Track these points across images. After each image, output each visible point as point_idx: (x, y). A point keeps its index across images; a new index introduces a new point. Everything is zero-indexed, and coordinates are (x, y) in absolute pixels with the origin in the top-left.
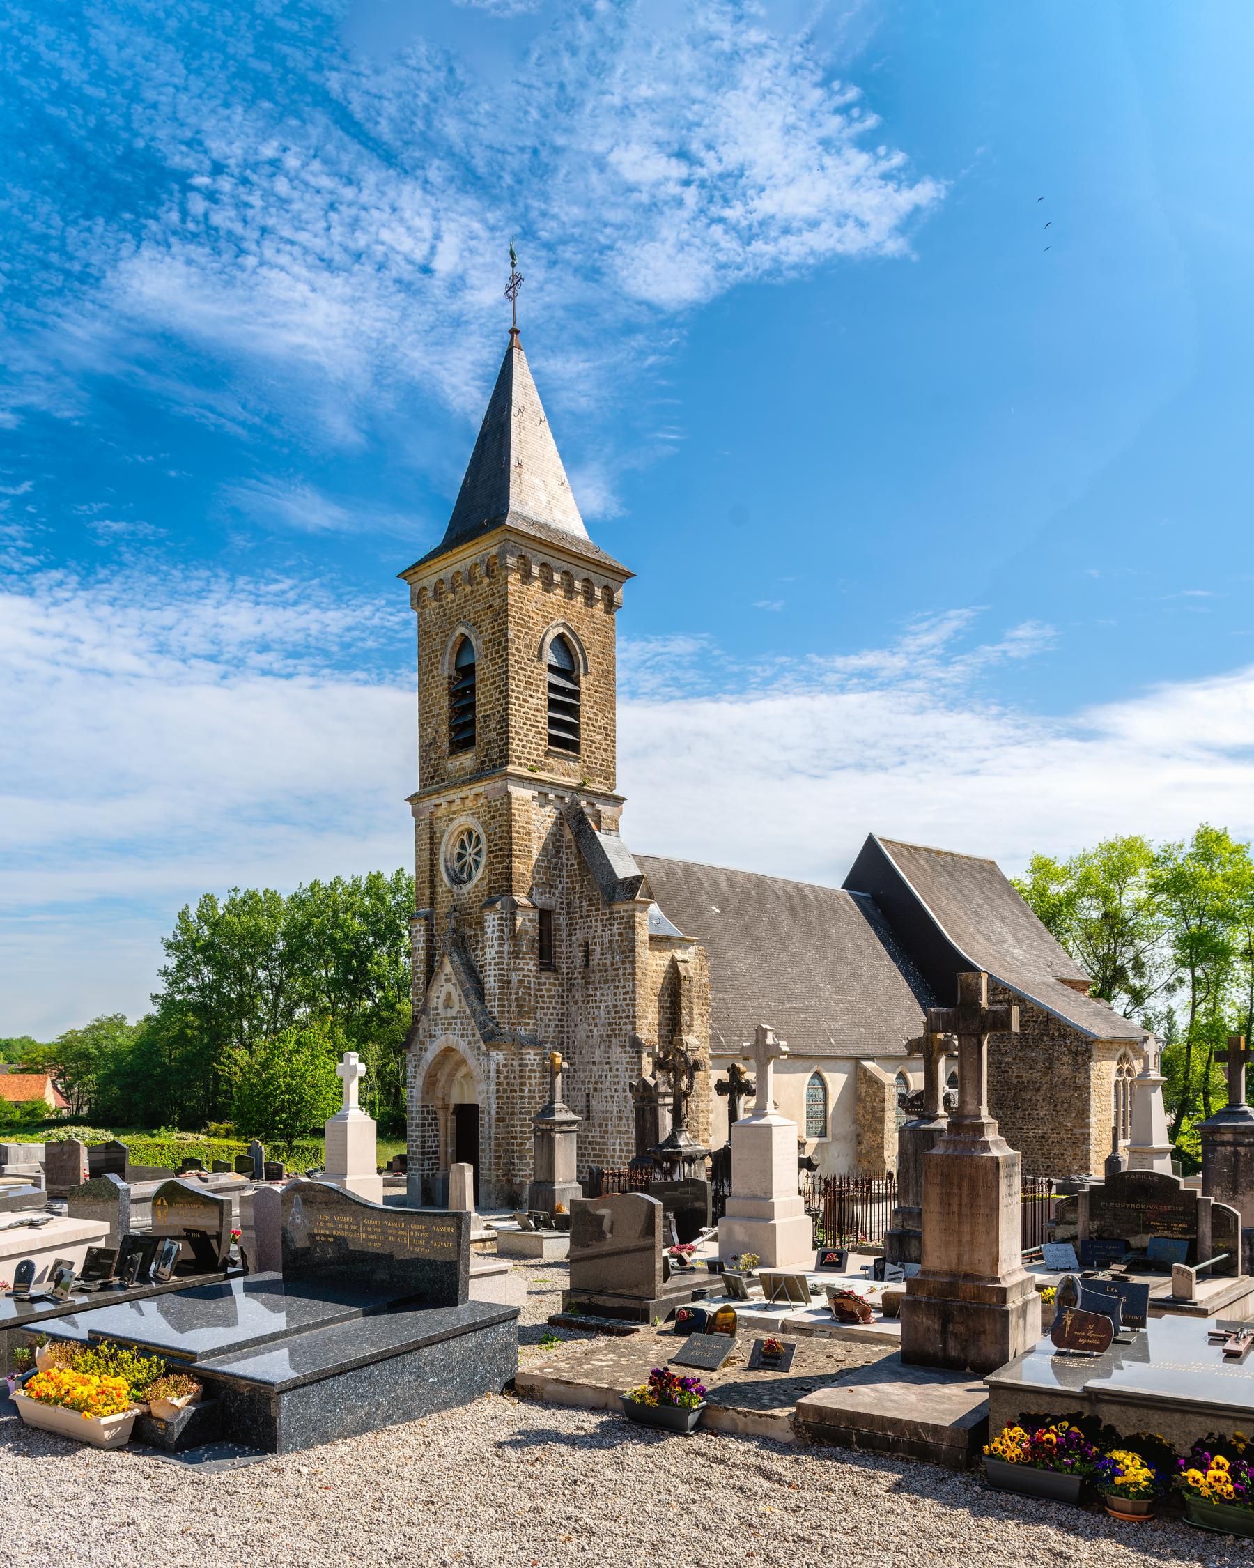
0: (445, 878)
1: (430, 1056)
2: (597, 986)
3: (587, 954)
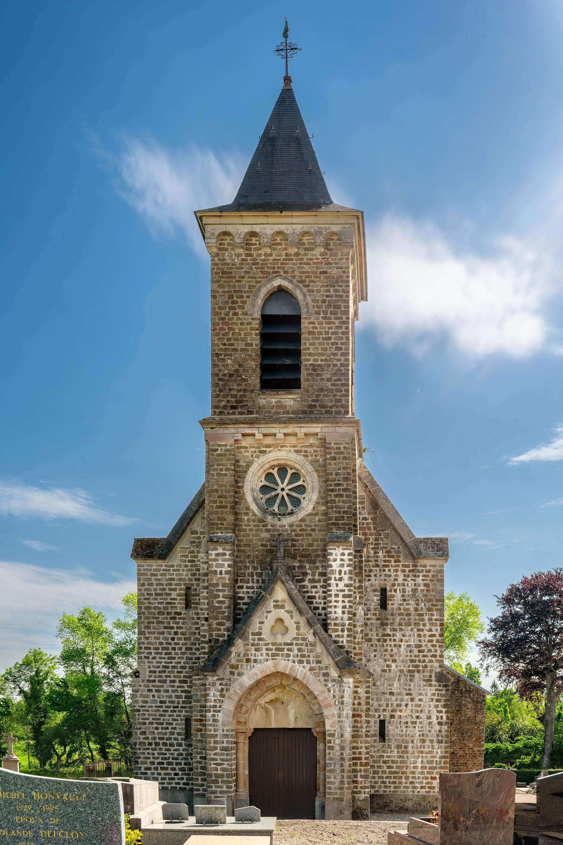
0: (254, 507)
2: (398, 628)
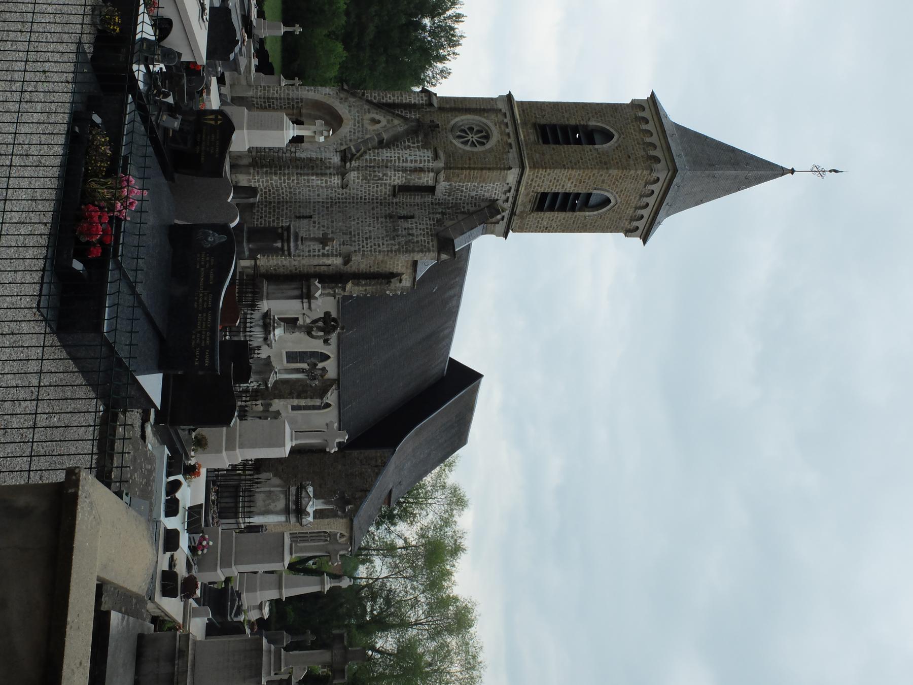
3: (406, 218)
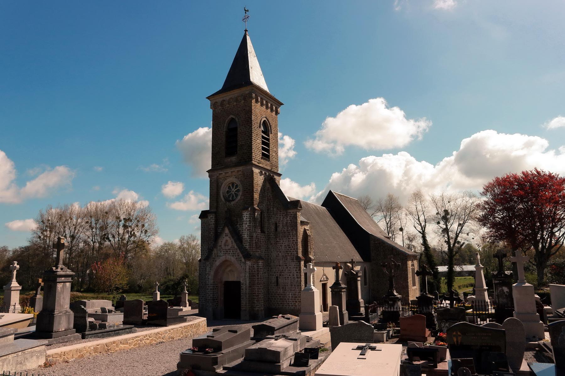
0: (223, 199)
1: (217, 263)
3: (276, 227)
